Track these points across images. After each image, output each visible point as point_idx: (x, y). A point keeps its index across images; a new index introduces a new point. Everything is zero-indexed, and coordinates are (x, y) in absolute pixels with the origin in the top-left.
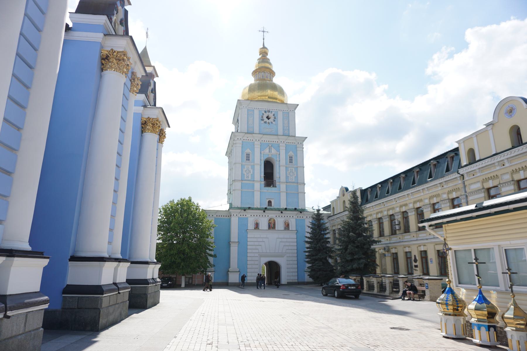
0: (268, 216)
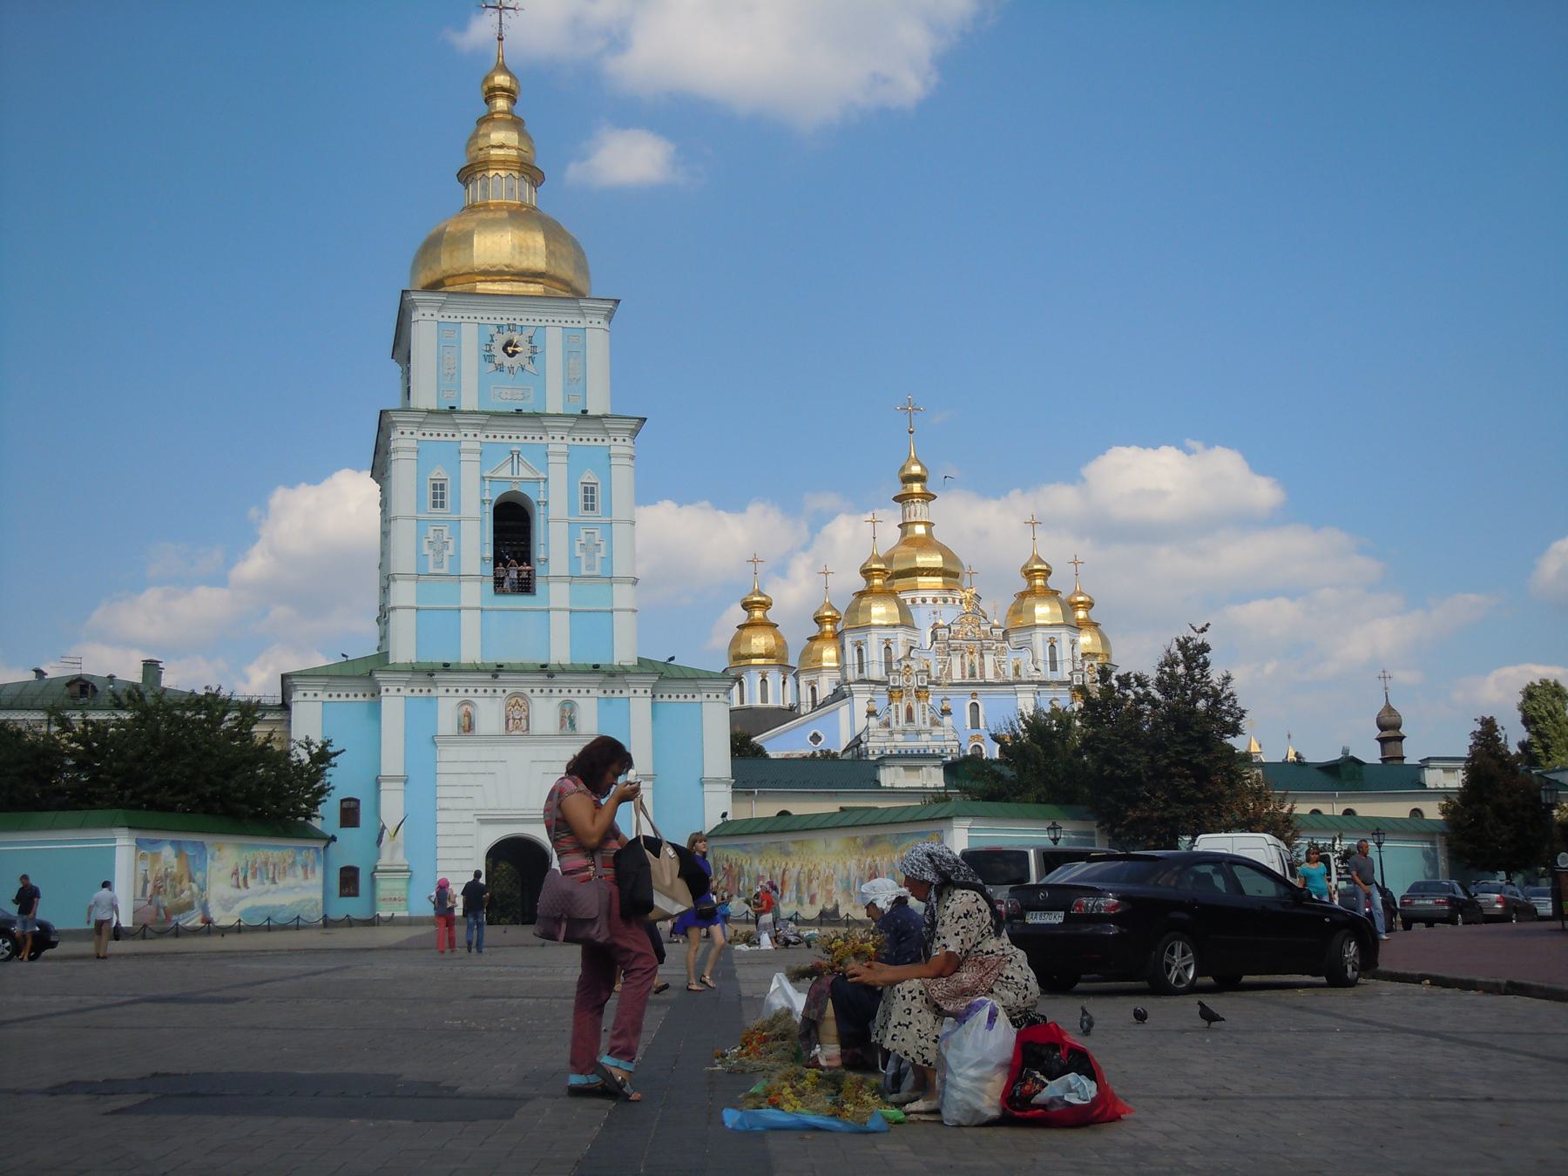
0: (504, 691)
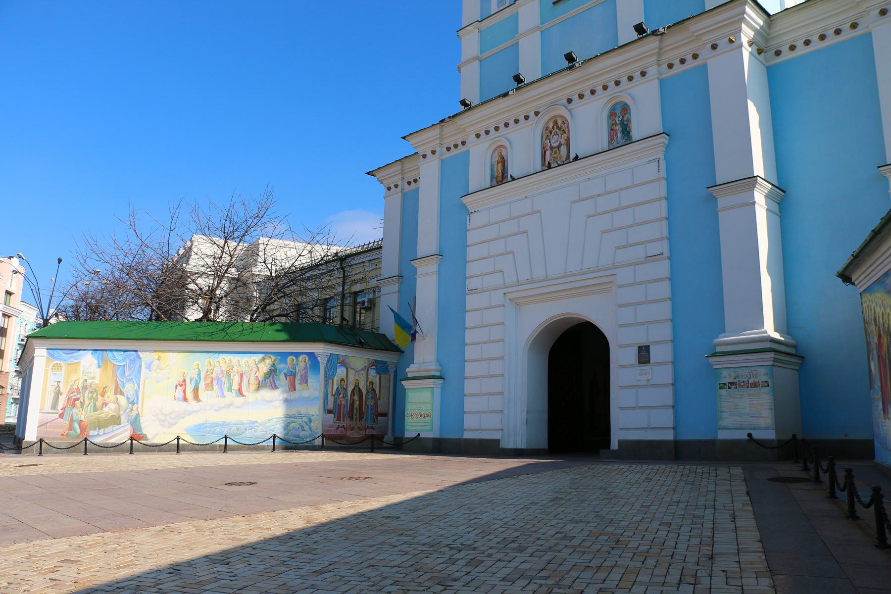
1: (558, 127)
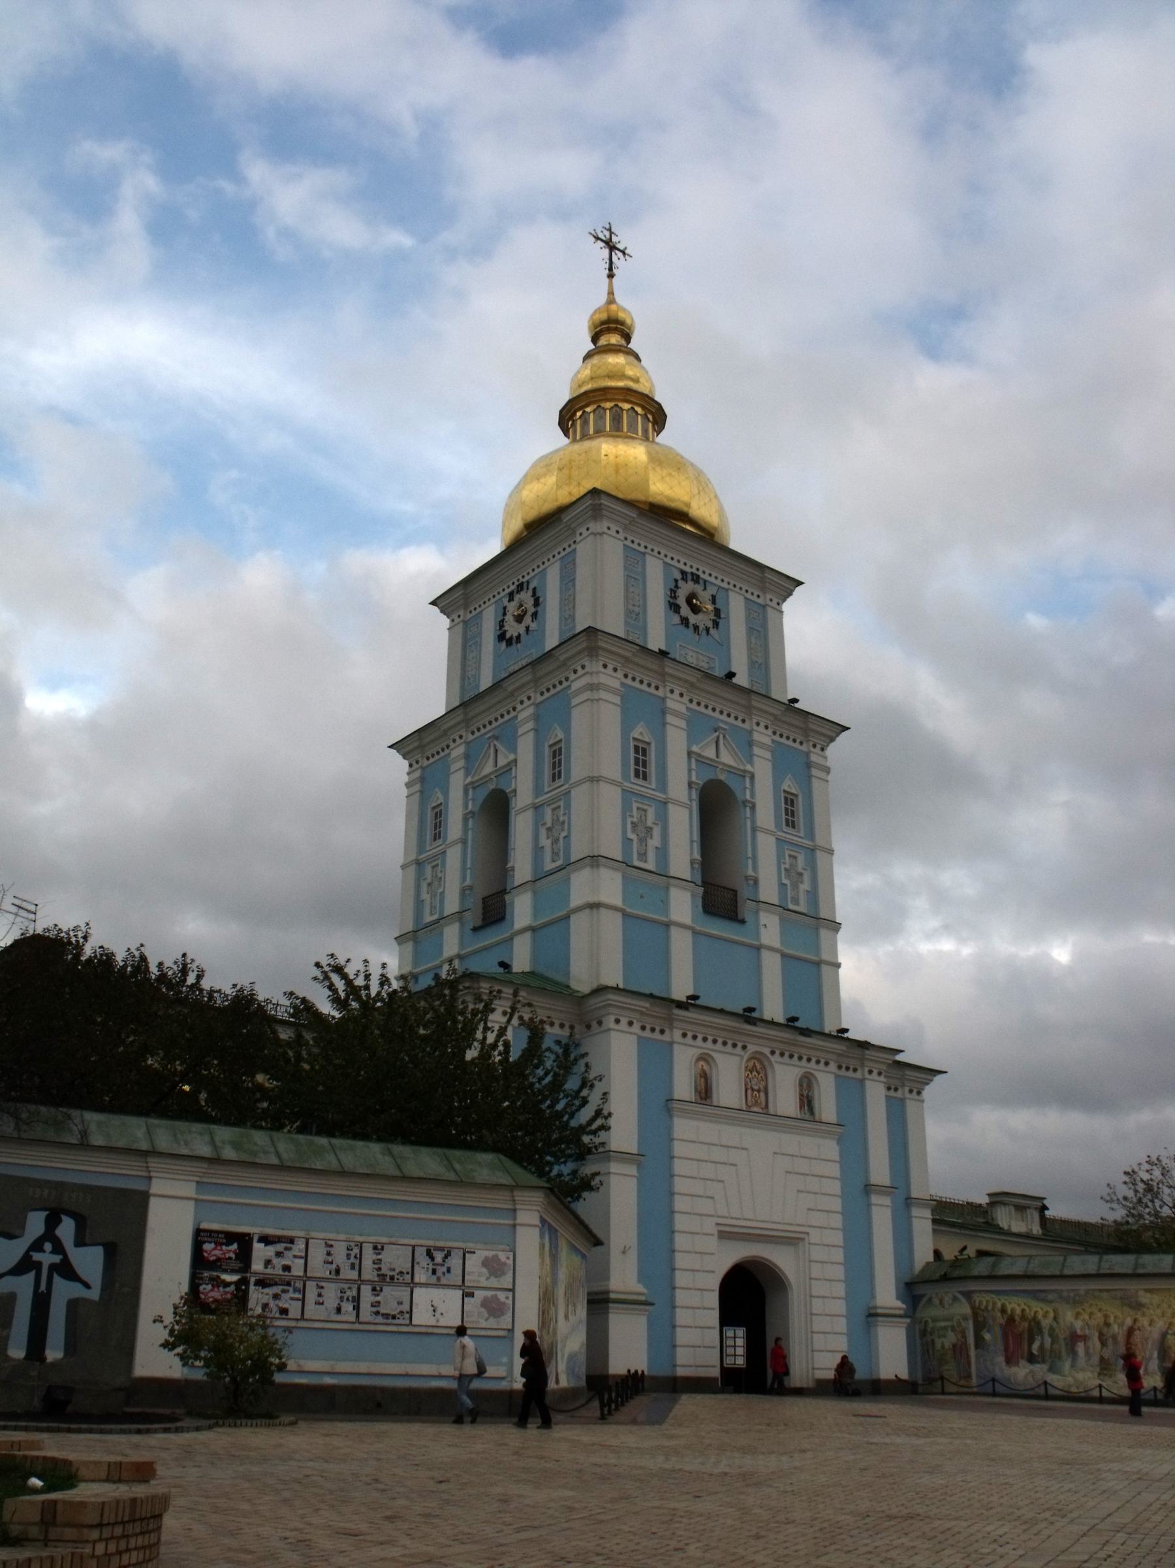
0: (744, 1047)
1: (757, 1071)
